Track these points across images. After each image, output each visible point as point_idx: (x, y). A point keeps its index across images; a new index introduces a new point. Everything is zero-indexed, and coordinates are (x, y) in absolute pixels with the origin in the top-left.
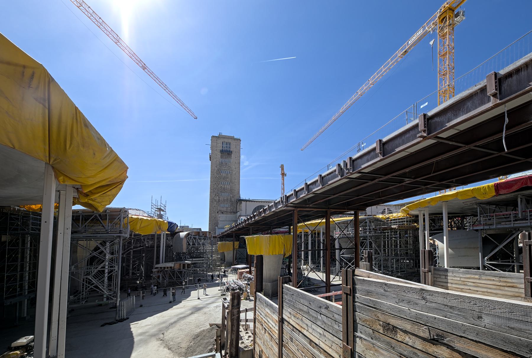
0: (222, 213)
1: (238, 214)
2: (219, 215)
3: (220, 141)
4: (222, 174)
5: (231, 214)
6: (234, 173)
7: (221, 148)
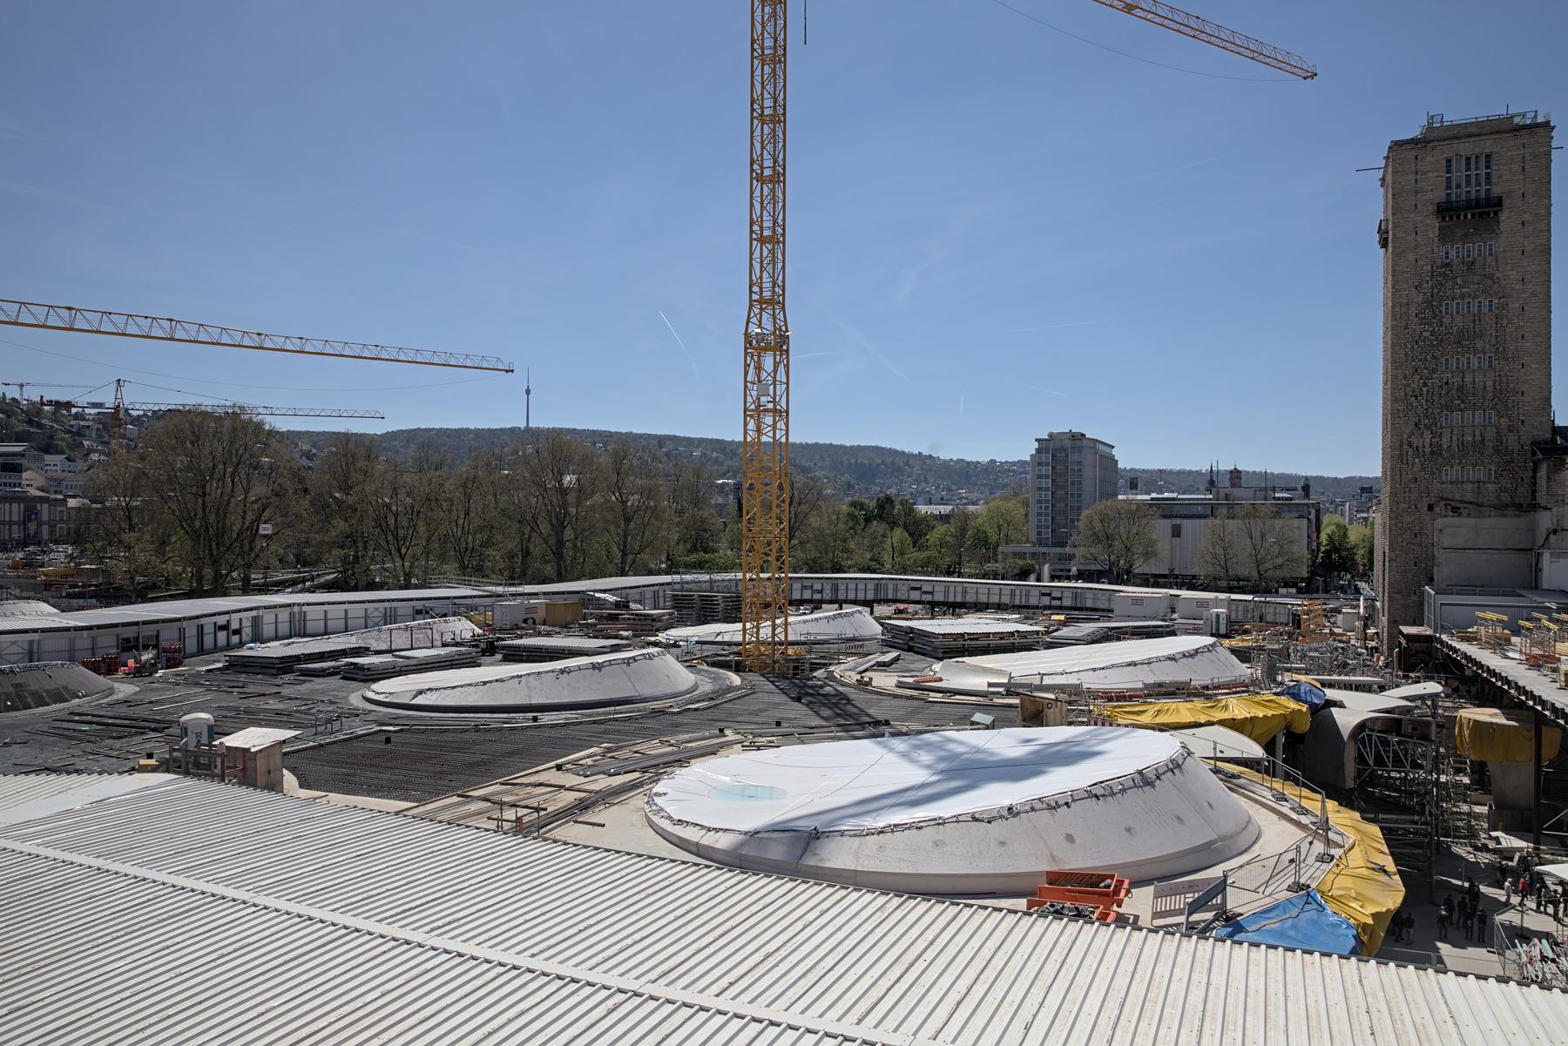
0: (1455, 510)
2: (1439, 522)
4: (1447, 320)
5: (1505, 515)
7: (1440, 195)
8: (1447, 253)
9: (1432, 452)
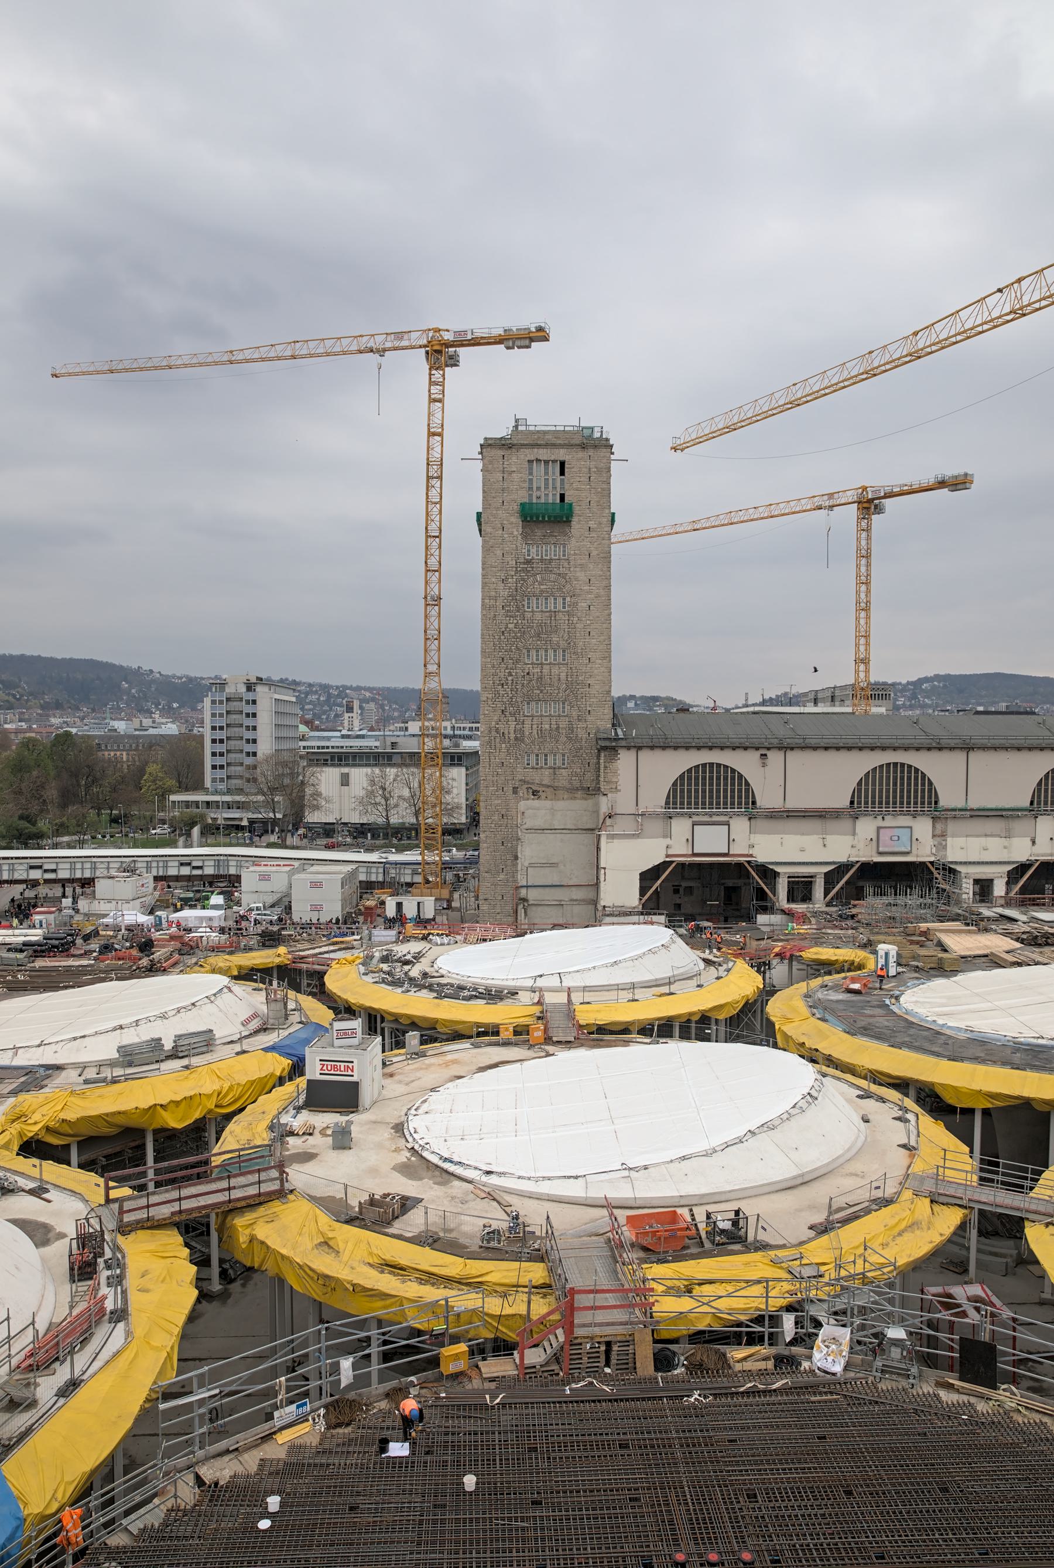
0: (535, 793)
1: (604, 805)
2: (523, 805)
3: (517, 460)
4: (528, 615)
5: (575, 798)
6: (583, 605)
7: (522, 496)
8: (529, 551)
9: (516, 739)
